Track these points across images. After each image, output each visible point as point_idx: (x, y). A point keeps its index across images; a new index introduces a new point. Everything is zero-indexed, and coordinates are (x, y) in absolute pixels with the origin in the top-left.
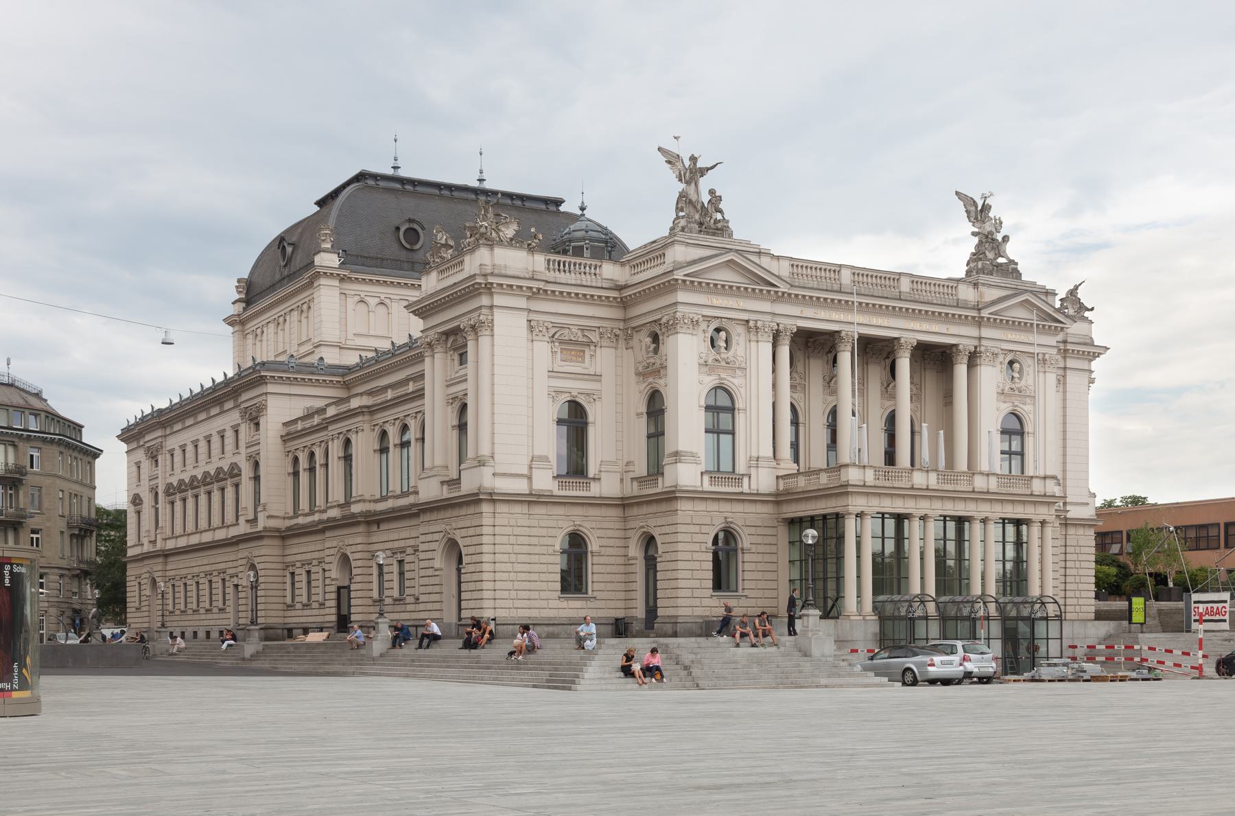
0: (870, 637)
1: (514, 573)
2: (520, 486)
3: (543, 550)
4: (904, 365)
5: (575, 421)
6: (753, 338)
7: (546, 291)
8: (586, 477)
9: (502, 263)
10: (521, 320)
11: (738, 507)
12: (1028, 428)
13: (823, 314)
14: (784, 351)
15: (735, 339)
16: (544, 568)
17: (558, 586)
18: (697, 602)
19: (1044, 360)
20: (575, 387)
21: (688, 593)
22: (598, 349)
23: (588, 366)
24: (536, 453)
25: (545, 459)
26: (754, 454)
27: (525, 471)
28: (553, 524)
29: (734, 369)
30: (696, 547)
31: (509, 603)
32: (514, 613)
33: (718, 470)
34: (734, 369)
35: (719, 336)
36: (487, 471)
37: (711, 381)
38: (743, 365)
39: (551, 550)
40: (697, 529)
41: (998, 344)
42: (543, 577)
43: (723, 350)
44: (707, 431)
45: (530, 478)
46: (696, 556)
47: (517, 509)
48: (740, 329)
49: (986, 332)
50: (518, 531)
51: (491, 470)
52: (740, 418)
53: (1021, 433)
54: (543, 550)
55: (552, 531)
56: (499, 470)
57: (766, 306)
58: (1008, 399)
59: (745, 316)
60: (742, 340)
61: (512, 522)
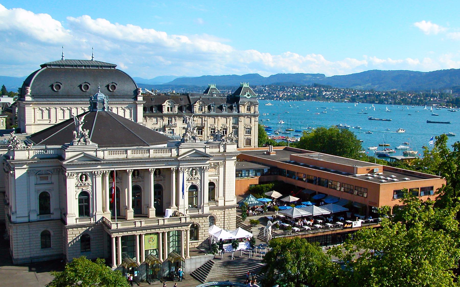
2: (26, 220)
17: (40, 247)
22: (53, 176)
23: (49, 181)
24: (31, 209)
25: (35, 210)
28: (38, 229)
32: (24, 257)
35: (83, 177)
43: (84, 181)
59: (91, 171)
61: (23, 231)
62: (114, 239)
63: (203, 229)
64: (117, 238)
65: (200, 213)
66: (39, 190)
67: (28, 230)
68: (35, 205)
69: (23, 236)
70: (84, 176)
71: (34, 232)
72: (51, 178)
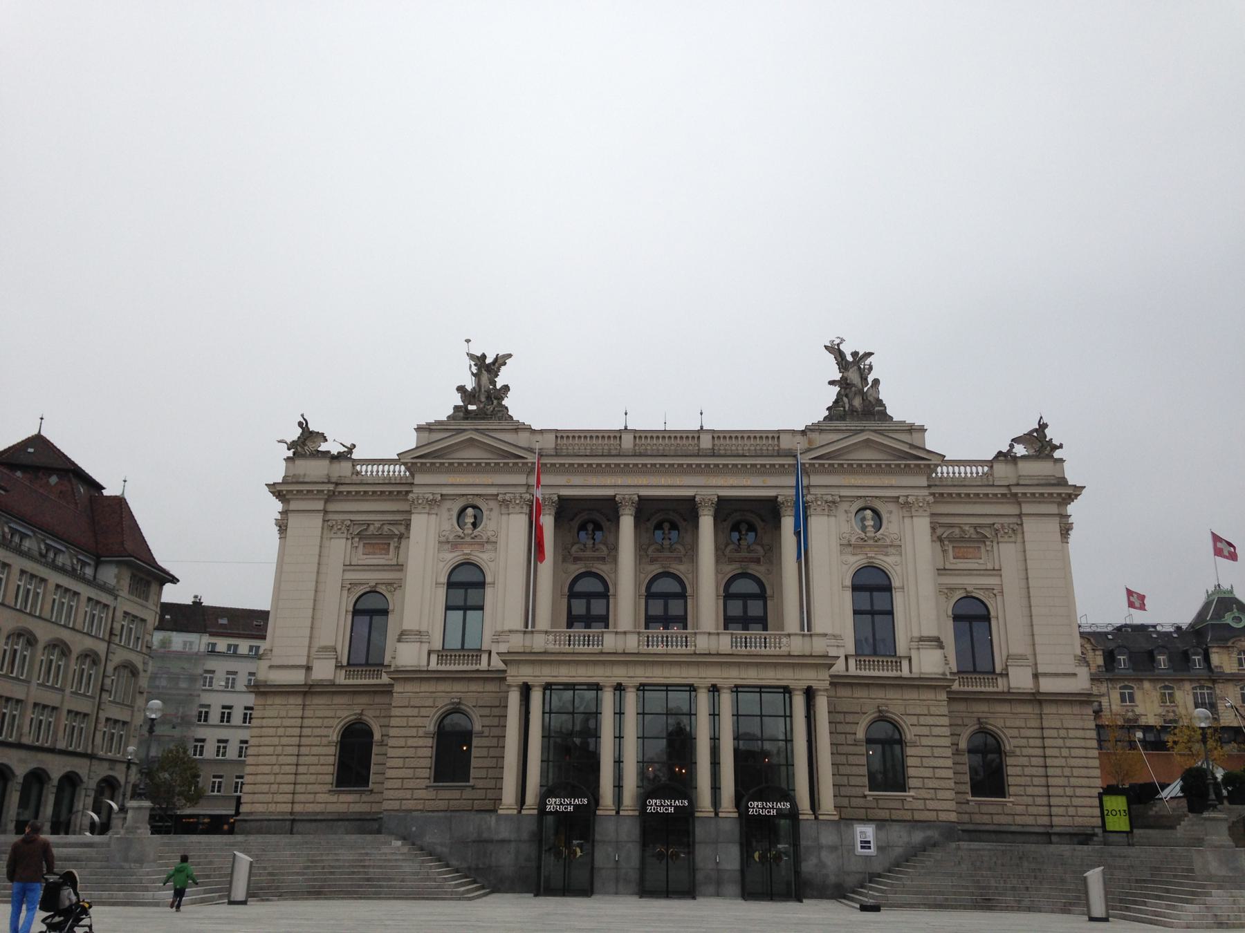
0: (525, 836)
1: (282, 764)
2: (298, 677)
3: (317, 741)
4: (706, 523)
5: (370, 611)
6: (504, 510)
7: (340, 492)
8: (382, 665)
9: (302, 473)
10: (317, 521)
11: (474, 687)
12: (896, 583)
13: (594, 480)
14: (547, 522)
15: (485, 513)
16: (314, 760)
18: (408, 794)
19: (907, 503)
20: (372, 577)
21: (398, 784)
26: (499, 629)
27: (304, 663)
28: (331, 714)
29: (482, 544)
30: (413, 732)
31: (268, 798)
32: (272, 808)
33: (463, 648)
34: (482, 544)
36: (264, 664)
37: (453, 557)
38: (493, 539)
39: (325, 741)
40: (415, 712)
41: (835, 491)
42: (313, 769)
44: (448, 608)
45: (308, 668)
46: (411, 742)
47: (293, 700)
48: (492, 504)
49: (815, 480)
50: (287, 722)
51: (267, 663)
52: (489, 591)
53: (888, 588)
54: (317, 741)
55: (328, 723)
56: (276, 662)
57: (521, 479)
58: (859, 551)
59: (494, 491)
60: (494, 514)
61: (283, 714)
62: (514, 698)
63: (925, 741)
64: (526, 690)
65: (905, 672)
66: (354, 584)
67: (300, 714)
68: (335, 628)
69: (281, 731)
70: (470, 511)
71: (318, 722)
72: (398, 548)
